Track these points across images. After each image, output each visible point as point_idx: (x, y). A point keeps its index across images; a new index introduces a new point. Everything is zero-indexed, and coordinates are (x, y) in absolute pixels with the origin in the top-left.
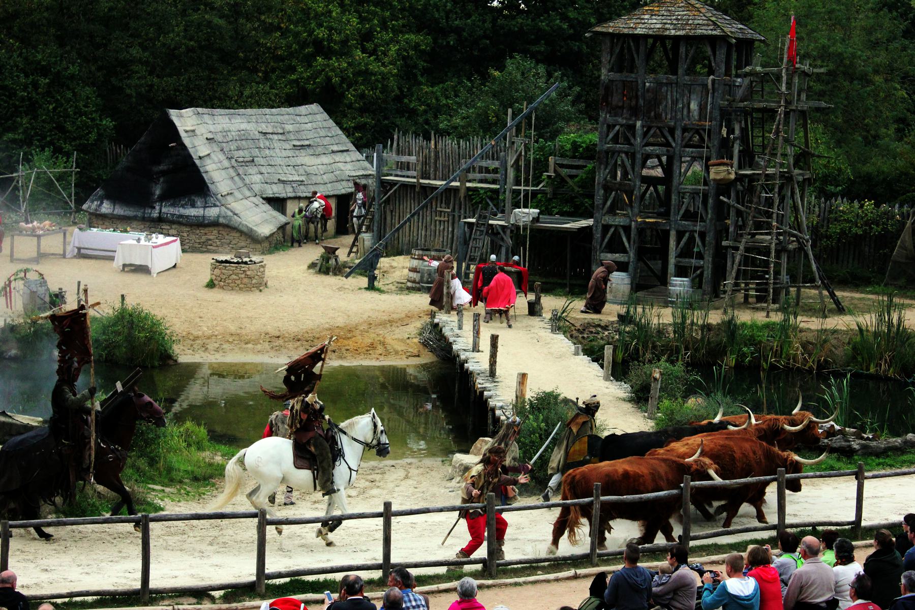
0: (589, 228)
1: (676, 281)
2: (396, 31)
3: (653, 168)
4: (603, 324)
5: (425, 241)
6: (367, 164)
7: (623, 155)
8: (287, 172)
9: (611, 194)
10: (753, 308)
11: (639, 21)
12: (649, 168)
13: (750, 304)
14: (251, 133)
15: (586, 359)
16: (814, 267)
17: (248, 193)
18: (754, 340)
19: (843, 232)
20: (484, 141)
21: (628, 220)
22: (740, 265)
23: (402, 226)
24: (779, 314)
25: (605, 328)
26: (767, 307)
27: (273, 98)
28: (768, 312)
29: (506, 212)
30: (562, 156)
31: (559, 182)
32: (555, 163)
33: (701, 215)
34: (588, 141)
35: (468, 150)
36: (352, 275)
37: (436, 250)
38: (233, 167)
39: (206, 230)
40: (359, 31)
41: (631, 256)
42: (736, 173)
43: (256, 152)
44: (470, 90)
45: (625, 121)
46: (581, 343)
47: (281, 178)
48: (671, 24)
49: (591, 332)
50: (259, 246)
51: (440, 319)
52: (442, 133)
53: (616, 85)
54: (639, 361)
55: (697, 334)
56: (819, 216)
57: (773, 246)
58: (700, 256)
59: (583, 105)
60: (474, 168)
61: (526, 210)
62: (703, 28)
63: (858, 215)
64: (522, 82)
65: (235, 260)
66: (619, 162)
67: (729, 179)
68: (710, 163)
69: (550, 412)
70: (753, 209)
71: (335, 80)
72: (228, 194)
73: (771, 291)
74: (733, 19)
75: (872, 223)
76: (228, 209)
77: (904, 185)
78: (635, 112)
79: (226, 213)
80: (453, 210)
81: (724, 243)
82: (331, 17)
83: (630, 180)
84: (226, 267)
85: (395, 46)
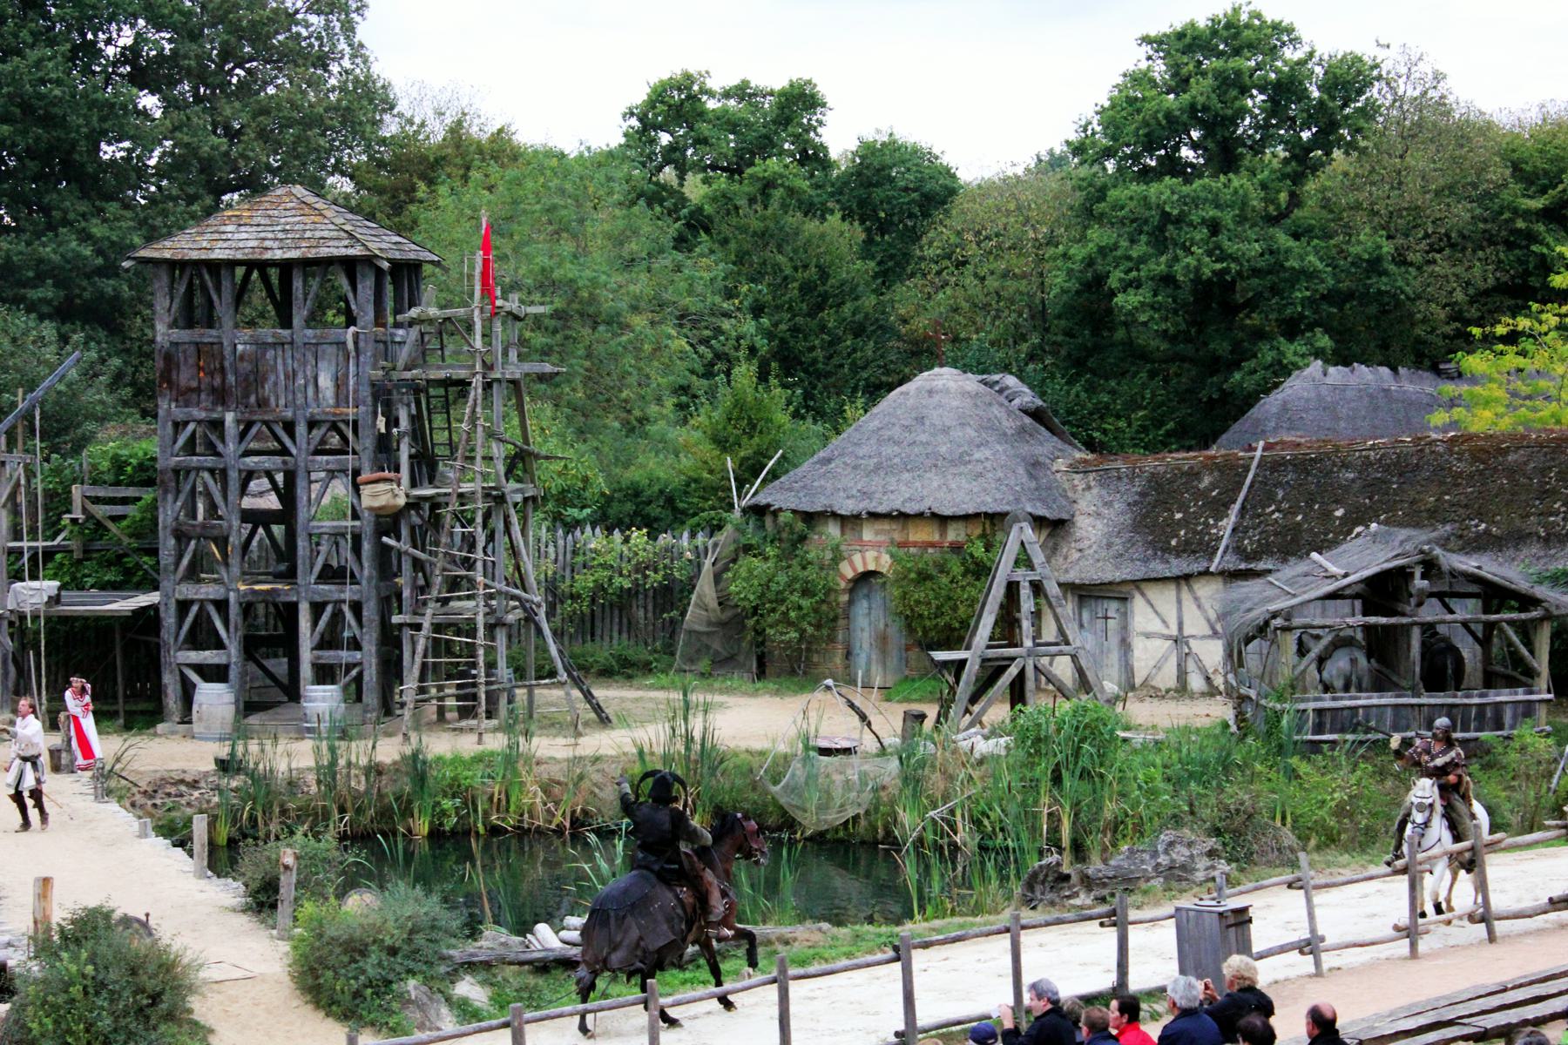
0: (155, 608)
3: (261, 494)
4: (189, 778)
7: (206, 475)
9: (188, 544)
11: (216, 236)
12: (254, 496)
15: (162, 843)
16: (553, 650)
19: (600, 588)
21: (222, 590)
22: (425, 656)
24: (500, 735)
25: (194, 785)
30: (94, 483)
34: (141, 454)
41: (232, 654)
42: (407, 496)
45: (203, 415)
46: (151, 816)
49: (169, 795)
53: (184, 352)
54: (256, 838)
56: (556, 561)
57: (480, 620)
58: (355, 645)
59: (129, 389)
61: (35, 584)
64: (12, 354)
68: (359, 479)
73: (483, 697)
75: (647, 568)
77: (695, 500)
78: (221, 396)
81: (396, 619)
83: (220, 518)
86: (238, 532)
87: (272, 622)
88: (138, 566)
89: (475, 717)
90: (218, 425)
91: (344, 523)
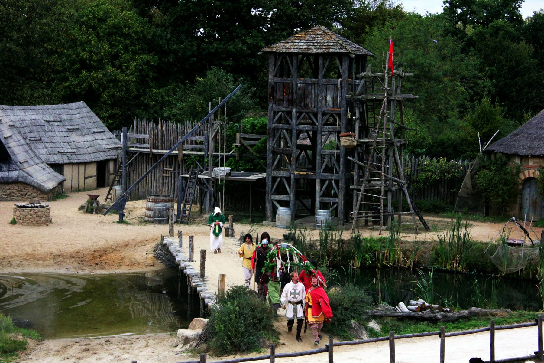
0: (264, 179)
1: (321, 212)
2: (134, 53)
3: (304, 139)
5: (157, 190)
6: (116, 140)
7: (285, 131)
8: (63, 146)
9: (277, 156)
10: (371, 229)
11: (292, 44)
12: (301, 139)
13: (369, 226)
14: (39, 122)
16: (409, 201)
17: (38, 161)
18: (372, 249)
19: (427, 178)
20: (194, 124)
22: (361, 201)
23: (140, 180)
24: (388, 232)
26: (380, 228)
27: (53, 98)
28: (381, 231)
29: (209, 169)
30: (245, 132)
31: (243, 149)
32: (240, 137)
33: (336, 169)
34: (261, 122)
35: (183, 130)
36: (109, 213)
37: (164, 196)
38: (27, 144)
39: (10, 186)
40: (110, 53)
42: (357, 142)
43: (42, 134)
44: (184, 91)
45: (285, 109)
47: (59, 150)
48: (313, 45)
50: (45, 196)
51: (167, 241)
52: (166, 119)
53: (279, 86)
55: (335, 246)
56: (411, 168)
57: (382, 188)
58: (336, 196)
59: (258, 99)
60: (187, 141)
61: (222, 168)
62: (334, 47)
63: (436, 167)
64: (217, 85)
65: (30, 205)
66: (282, 136)
67: (353, 145)
68: (340, 135)
69: (241, 299)
70: (369, 164)
71: (95, 86)
72: (24, 162)
73: (382, 217)
74: (353, 42)
75: (445, 172)
76: (24, 171)
77: (465, 148)
78: (291, 103)
79: (23, 174)
80: (175, 169)
81: (351, 187)
82: (91, 44)
84: (23, 210)
85: (133, 63)
86: (295, 152)
87: (306, 186)
88: (259, 163)
89: (379, 225)
90: (290, 113)
91: (334, 151)
